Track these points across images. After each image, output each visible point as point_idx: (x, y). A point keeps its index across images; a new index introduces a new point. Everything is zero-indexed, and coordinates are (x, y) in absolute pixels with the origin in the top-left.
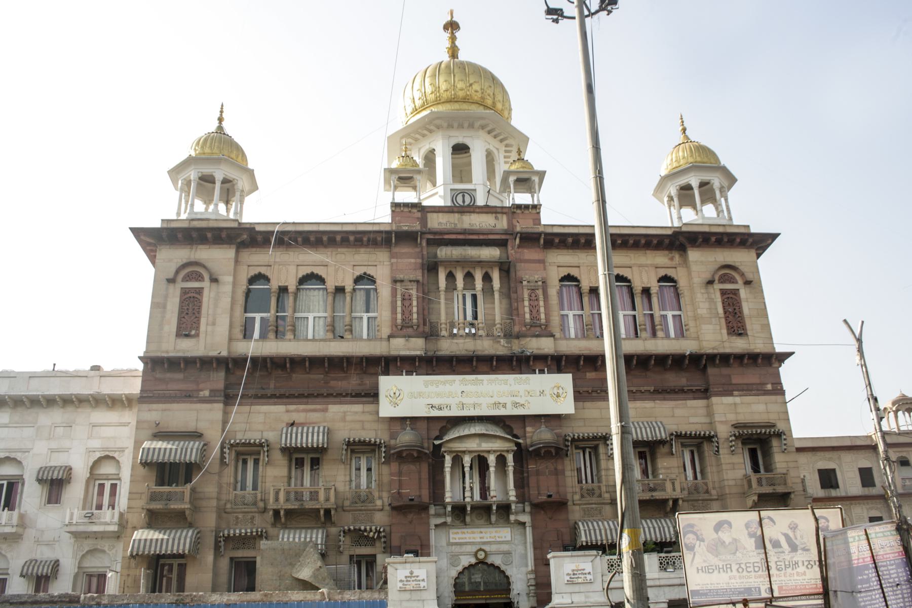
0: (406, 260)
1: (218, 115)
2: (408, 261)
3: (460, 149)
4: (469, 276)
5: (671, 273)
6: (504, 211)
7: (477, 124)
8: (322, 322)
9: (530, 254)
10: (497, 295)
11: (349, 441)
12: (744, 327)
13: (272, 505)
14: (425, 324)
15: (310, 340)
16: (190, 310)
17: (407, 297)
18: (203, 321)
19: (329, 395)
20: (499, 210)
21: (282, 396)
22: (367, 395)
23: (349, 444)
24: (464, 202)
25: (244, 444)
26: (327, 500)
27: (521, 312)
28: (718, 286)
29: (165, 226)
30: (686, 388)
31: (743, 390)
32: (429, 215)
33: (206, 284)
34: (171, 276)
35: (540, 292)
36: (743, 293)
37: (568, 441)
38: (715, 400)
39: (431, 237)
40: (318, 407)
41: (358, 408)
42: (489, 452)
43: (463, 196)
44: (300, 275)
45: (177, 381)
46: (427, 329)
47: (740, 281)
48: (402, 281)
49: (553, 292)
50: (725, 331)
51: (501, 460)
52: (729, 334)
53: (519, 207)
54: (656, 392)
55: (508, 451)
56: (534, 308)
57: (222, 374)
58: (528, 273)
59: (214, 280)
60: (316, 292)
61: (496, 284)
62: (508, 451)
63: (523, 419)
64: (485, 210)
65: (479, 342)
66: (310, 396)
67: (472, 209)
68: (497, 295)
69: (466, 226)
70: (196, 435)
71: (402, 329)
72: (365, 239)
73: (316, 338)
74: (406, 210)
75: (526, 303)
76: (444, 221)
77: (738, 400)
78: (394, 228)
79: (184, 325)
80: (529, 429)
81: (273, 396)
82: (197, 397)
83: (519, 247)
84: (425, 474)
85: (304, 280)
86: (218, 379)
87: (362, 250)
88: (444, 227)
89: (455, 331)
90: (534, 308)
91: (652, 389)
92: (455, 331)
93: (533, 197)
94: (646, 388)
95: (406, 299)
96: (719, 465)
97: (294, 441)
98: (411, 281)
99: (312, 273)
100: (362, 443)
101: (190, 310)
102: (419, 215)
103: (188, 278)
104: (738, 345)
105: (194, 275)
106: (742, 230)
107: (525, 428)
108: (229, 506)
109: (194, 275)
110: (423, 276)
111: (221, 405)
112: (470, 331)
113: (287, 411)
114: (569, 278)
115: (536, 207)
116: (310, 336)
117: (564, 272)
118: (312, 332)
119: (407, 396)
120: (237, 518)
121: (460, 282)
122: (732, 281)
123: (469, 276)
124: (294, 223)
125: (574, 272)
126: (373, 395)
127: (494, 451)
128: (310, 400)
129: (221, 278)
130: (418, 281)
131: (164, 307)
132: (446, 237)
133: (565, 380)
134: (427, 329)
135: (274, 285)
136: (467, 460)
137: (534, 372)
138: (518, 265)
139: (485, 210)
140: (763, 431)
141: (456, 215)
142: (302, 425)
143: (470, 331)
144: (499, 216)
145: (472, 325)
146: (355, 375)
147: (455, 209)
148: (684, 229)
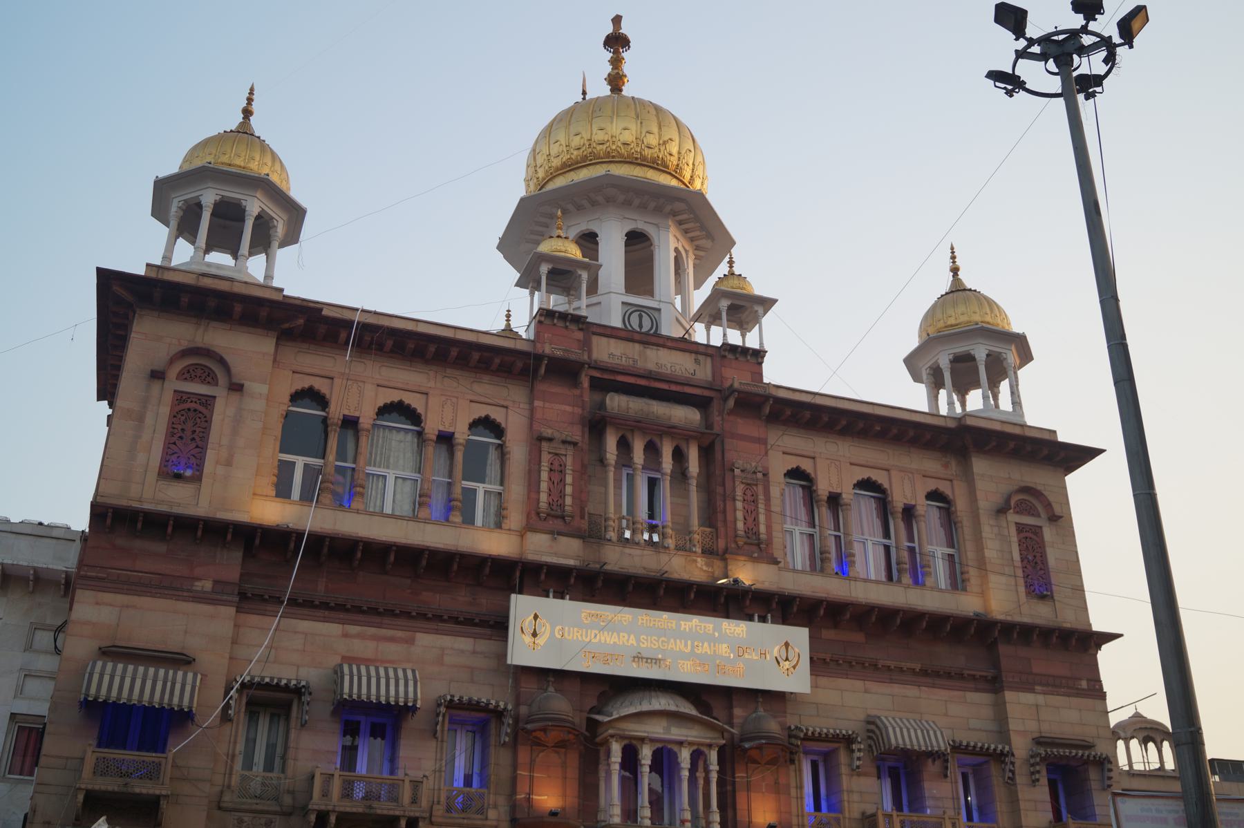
0: (557, 406)
1: (244, 103)
2: (560, 410)
3: (636, 239)
4: (652, 450)
5: (944, 488)
6: (710, 351)
7: (668, 208)
8: (408, 487)
9: (746, 427)
10: (693, 488)
11: (451, 701)
12: (1048, 585)
13: (317, 802)
14: (582, 517)
15: (388, 516)
16: (188, 433)
17: (556, 466)
18: (210, 456)
19: (423, 616)
20: (702, 349)
21: (341, 608)
22: (483, 624)
23: (451, 705)
24: (641, 326)
25: (268, 686)
26: (414, 801)
27: (730, 517)
28: (1013, 517)
29: (153, 275)
30: (966, 672)
31: (1047, 685)
32: (595, 339)
33: (220, 392)
34: (158, 366)
35: (760, 489)
36: (1048, 533)
37: (796, 737)
38: (1009, 696)
39: (597, 374)
40: (399, 634)
41: (464, 644)
42: (681, 743)
43: (641, 317)
44: (381, 404)
45: (152, 557)
46: (584, 525)
47: (1043, 515)
48: (550, 440)
49: (775, 491)
50: (1022, 589)
51: (697, 756)
52: (1028, 594)
53: (733, 349)
54: (924, 673)
55: (710, 746)
56: (752, 514)
57: (238, 555)
58: (740, 455)
59: (236, 388)
60: (401, 436)
61: (694, 466)
62: (710, 746)
63: (728, 694)
64: (682, 345)
65: (664, 558)
66: (390, 613)
67: (653, 339)
68: (694, 482)
69: (651, 366)
70: (181, 660)
71: (549, 518)
72: (497, 361)
73: (397, 513)
74: (561, 324)
75: (739, 505)
76: (618, 352)
77: (1041, 699)
78: (548, 349)
79: (174, 458)
80: (738, 712)
81: (325, 606)
82: (189, 591)
83: (731, 412)
84: (573, 772)
85: (385, 410)
86: (230, 564)
87: (486, 378)
88: (618, 362)
89: (628, 534)
90: (752, 514)
91: (918, 667)
92: (628, 534)
93: (743, 336)
94: (909, 665)
95: (558, 471)
96: (1014, 801)
97: (364, 690)
98: (564, 442)
99: (401, 403)
100: (473, 706)
101: (188, 433)
102: (580, 335)
103: (187, 375)
104: (1037, 613)
105: (199, 372)
106: (1047, 436)
107: (730, 708)
108: (227, 798)
109: (199, 372)
110: (583, 436)
111: (232, 610)
112: (651, 537)
113: (345, 635)
114: (795, 474)
115: (758, 355)
116: (388, 509)
117: (792, 463)
118: (391, 502)
119: (555, 634)
120: (241, 821)
121: (638, 456)
122: (1032, 512)
123: (652, 450)
124: (375, 313)
125: (806, 465)
126: (499, 626)
127: (691, 744)
128: (386, 620)
129: (247, 384)
130: (575, 444)
131: (141, 419)
132: (620, 378)
133: (799, 636)
134: (584, 525)
135: (336, 411)
136: (646, 754)
137: (751, 619)
138: (727, 441)
139: (682, 345)
140: (1080, 753)
141: (637, 345)
142: (368, 662)
143: (651, 537)
144: (700, 357)
145: (652, 529)
146: (479, 589)
147: (637, 337)
148: (970, 422)
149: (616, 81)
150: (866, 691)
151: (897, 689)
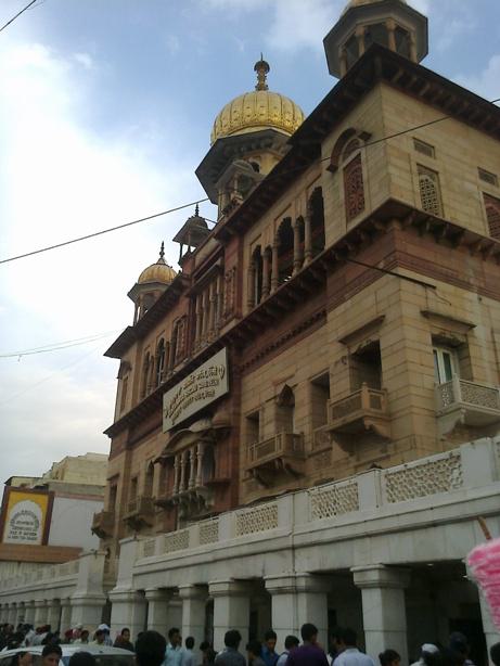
30: (314, 316)
54: (295, 333)
77: (348, 303)
149: (261, 87)
150: (274, 365)
151: (287, 353)
